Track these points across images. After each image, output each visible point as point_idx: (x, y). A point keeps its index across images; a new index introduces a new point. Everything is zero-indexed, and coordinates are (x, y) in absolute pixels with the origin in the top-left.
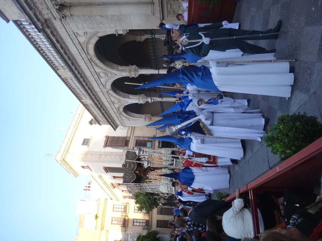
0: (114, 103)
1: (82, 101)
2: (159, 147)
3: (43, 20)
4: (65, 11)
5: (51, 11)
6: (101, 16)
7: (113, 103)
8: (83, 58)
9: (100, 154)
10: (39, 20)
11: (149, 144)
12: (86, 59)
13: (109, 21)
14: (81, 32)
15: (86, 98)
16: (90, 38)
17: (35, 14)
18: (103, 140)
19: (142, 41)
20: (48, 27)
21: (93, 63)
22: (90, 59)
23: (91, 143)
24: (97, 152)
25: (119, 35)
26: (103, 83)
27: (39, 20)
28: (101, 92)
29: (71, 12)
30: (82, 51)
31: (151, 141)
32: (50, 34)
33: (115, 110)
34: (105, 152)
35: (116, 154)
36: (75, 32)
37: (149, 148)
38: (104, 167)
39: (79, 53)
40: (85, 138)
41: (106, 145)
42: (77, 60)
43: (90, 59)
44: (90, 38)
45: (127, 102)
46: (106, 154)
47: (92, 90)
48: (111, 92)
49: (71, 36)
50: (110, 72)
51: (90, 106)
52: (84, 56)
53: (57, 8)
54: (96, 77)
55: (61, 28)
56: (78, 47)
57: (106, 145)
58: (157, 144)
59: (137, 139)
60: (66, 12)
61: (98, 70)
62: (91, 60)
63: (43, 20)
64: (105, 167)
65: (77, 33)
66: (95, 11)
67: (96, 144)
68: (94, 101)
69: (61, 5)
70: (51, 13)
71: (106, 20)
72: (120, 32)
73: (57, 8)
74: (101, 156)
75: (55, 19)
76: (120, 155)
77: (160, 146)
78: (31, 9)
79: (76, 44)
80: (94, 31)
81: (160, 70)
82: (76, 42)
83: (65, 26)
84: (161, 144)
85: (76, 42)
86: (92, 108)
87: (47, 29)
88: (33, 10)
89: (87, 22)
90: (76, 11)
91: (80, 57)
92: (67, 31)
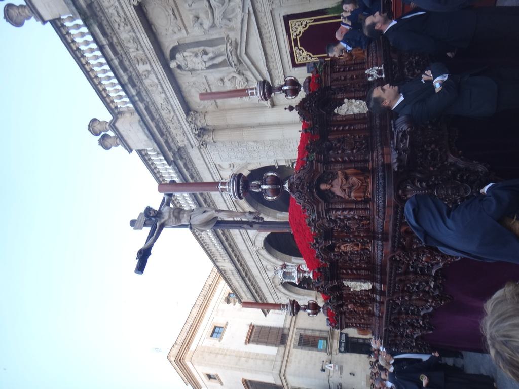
0: (267, 269)
1: (218, 264)
2: (340, 351)
3: (175, 149)
4: (206, 137)
6: (256, 142)
7: (265, 269)
8: (225, 200)
9: (239, 356)
10: (170, 149)
11: (322, 344)
13: (266, 148)
14: (225, 165)
15: (224, 260)
17: (167, 142)
18: (245, 330)
20: (182, 158)
22: (236, 201)
23: (227, 335)
24: (234, 351)
25: (280, 166)
26: (251, 237)
27: (170, 149)
28: (247, 251)
29: (214, 138)
31: (326, 339)
32: (183, 167)
33: (268, 281)
34: (246, 352)
35: (265, 358)
36: (217, 164)
37: (321, 351)
38: (243, 379)
40: (217, 325)
41: (249, 341)
42: (216, 204)
43: (236, 201)
46: (248, 356)
47: (235, 248)
48: (264, 252)
49: (211, 169)
51: (229, 272)
53: (197, 132)
55: (199, 159)
57: (249, 341)
58: (336, 344)
59: (302, 332)
60: (208, 138)
63: (175, 149)
64: (245, 380)
65: (219, 165)
66: (247, 134)
67: (233, 337)
68: (235, 265)
69: (201, 129)
70: (188, 139)
72: (282, 163)
73: (197, 132)
74: (239, 360)
75: (192, 147)
76: (272, 360)
77: (342, 349)
78: (162, 134)
80: (244, 162)
83: (204, 156)
84: (343, 345)
86: (231, 277)
87: (179, 161)
88: (165, 137)
89: (235, 150)
90: (220, 137)
92: (206, 162)
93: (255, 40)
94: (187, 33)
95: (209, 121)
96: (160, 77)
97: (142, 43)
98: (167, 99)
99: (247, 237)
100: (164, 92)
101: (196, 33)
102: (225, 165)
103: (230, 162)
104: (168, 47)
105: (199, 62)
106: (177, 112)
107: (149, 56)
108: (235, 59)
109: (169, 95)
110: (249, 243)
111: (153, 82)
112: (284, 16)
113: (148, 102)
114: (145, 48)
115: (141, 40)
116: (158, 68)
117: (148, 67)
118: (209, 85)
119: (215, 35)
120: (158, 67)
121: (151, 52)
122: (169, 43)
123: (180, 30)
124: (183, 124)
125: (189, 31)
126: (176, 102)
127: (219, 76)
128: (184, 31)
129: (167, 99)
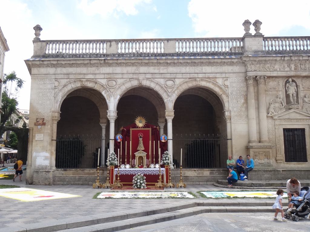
5: (253, 71)
12: (196, 76)
13: (239, 108)
16: (221, 88)
19: (158, 123)
21: (187, 80)
28: (137, 72)
29: (251, 85)
30: (207, 76)
32: (232, 61)
36: (228, 79)
39: (205, 73)
44: (221, 88)
45: (110, 96)
49: (225, 74)
50: (174, 92)
52: (201, 76)
54: (168, 76)
56: (211, 74)
61: (178, 81)
62: (195, 79)
70: (251, 71)
71: (240, 106)
79: (215, 74)
81: (172, 140)
82: (218, 75)
83: (235, 74)
85: (218, 75)
89: (238, 92)
91: (197, 71)
93: (298, 116)
94: (301, 90)
95: (262, 86)
96: (288, 72)
97: (304, 72)
98: (276, 70)
99: (157, 77)
100: (280, 71)
101: (301, 94)
102: (227, 83)
103: (229, 86)
104: (297, 80)
105: (293, 92)
106: (269, 72)
107: (299, 72)
108: (295, 107)
109: (278, 72)
110: (148, 76)
111: (286, 68)
112: (304, 129)
113: (277, 62)
114: (302, 72)
115: (305, 72)
116: (292, 74)
117: (293, 69)
118: (277, 91)
119: (300, 101)
120: (293, 74)
121: (299, 74)
122: (298, 81)
123: (303, 88)
124: (262, 73)
125: (302, 91)
126: (275, 74)
127: (281, 97)
128: (303, 89)
129: (276, 70)
